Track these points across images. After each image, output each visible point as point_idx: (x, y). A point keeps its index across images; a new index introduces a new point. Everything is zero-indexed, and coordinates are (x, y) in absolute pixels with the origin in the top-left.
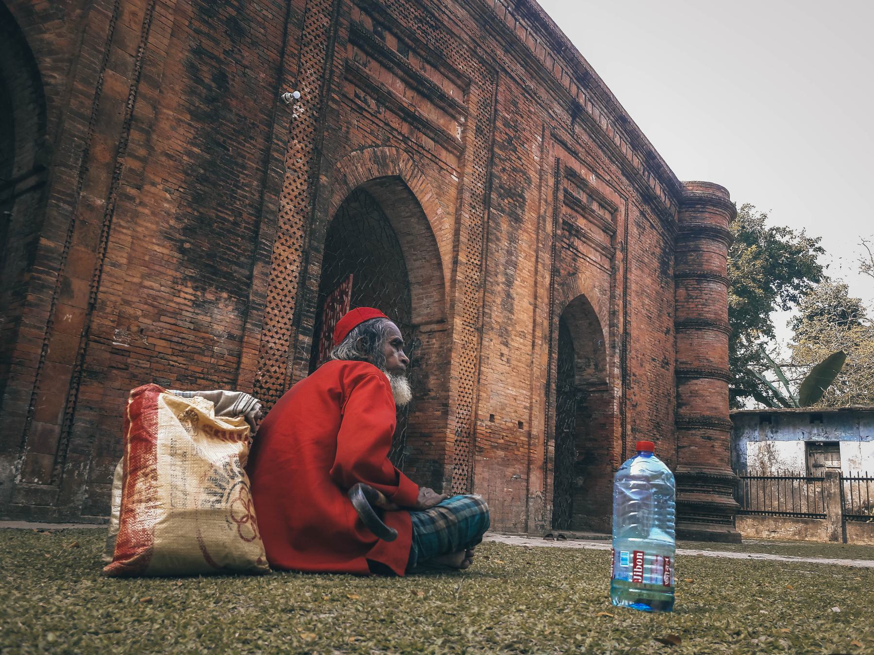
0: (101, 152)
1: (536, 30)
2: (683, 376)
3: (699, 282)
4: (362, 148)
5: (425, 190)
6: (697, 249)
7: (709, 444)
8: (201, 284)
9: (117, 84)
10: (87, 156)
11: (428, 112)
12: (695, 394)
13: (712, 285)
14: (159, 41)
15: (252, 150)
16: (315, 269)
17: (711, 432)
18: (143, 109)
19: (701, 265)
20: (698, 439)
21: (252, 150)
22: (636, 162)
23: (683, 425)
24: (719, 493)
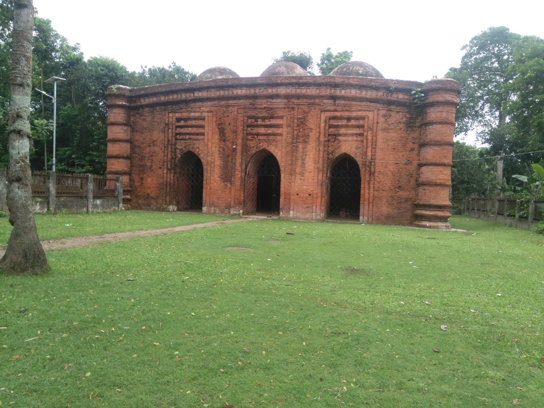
0: (209, 169)
1: (309, 86)
2: (420, 165)
3: (425, 126)
4: (254, 147)
5: (272, 149)
6: (426, 113)
7: (424, 191)
8: (224, 182)
9: (209, 159)
10: (207, 170)
11: (270, 131)
12: (422, 173)
13: (430, 127)
14: (213, 149)
15: (230, 159)
16: (243, 174)
17: (425, 187)
18: (213, 160)
19: (426, 119)
20: (421, 190)
21: (230, 159)
22: (380, 94)
23: (419, 184)
24: (426, 210)
